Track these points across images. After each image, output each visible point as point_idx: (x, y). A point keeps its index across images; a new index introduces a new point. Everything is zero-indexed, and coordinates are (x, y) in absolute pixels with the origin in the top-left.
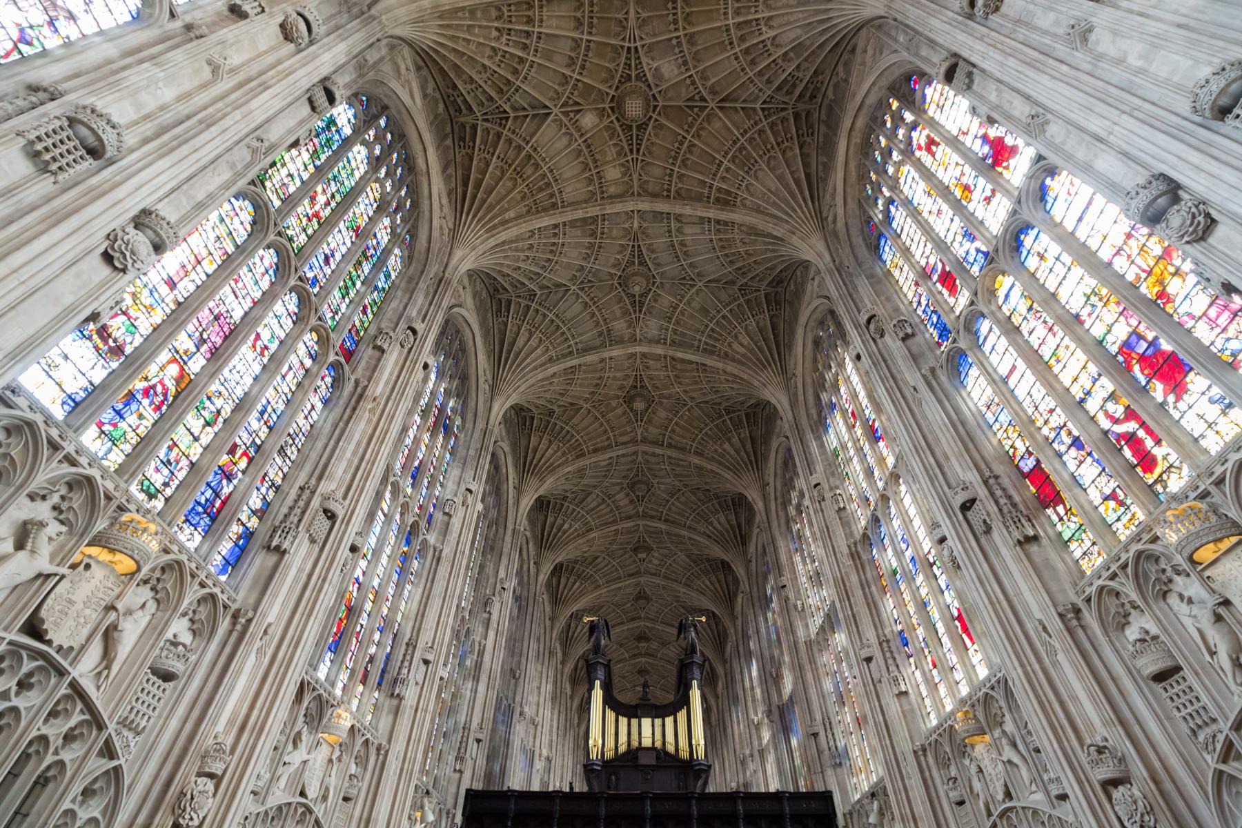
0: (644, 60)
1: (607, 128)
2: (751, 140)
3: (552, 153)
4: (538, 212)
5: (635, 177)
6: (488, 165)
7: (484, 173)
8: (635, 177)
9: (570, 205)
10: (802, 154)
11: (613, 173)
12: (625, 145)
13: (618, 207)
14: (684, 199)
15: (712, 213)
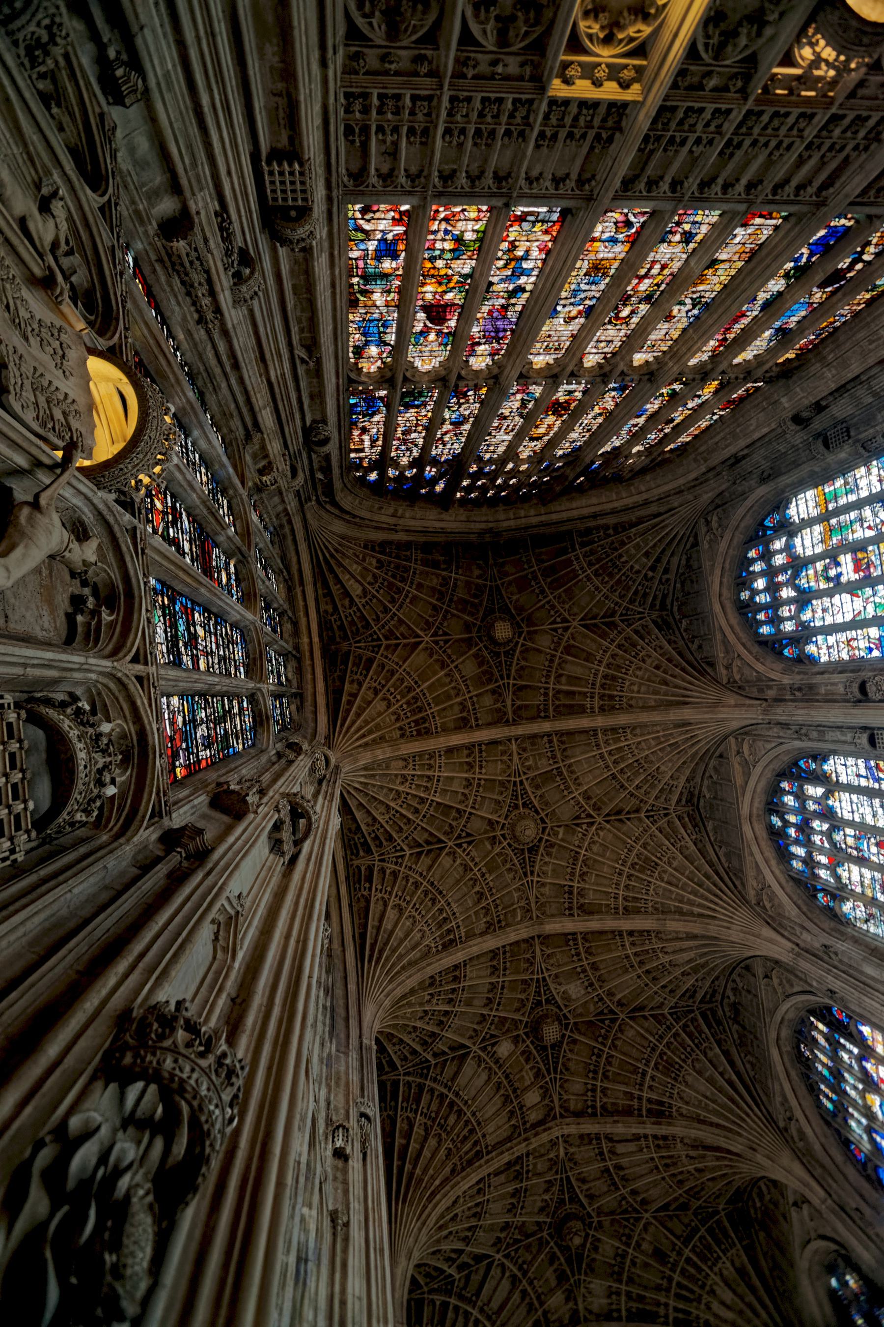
0: (552, 986)
1: (523, 1053)
2: (668, 1045)
3: (473, 1093)
4: (463, 1169)
5: (556, 1098)
6: (411, 1125)
7: (408, 1135)
8: (556, 1098)
9: (494, 1147)
10: (722, 1051)
11: (532, 1098)
12: (542, 1066)
13: (545, 1137)
14: (611, 1114)
15: (650, 1129)
